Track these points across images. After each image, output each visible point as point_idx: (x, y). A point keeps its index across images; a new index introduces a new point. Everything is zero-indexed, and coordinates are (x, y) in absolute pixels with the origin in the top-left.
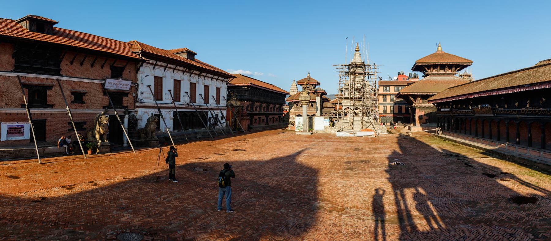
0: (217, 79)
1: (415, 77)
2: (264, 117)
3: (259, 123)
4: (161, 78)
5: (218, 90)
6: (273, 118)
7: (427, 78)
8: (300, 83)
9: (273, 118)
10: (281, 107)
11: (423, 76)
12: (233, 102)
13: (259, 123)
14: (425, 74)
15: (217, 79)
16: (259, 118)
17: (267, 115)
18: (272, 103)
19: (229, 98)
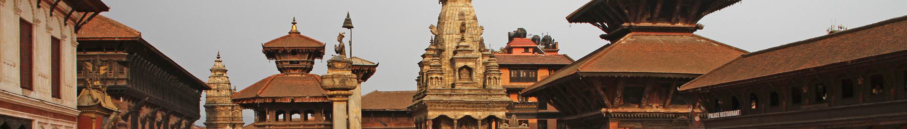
1: (549, 44)
7: (628, 37)
11: (602, 37)
12: (96, 94)
14: (604, 29)
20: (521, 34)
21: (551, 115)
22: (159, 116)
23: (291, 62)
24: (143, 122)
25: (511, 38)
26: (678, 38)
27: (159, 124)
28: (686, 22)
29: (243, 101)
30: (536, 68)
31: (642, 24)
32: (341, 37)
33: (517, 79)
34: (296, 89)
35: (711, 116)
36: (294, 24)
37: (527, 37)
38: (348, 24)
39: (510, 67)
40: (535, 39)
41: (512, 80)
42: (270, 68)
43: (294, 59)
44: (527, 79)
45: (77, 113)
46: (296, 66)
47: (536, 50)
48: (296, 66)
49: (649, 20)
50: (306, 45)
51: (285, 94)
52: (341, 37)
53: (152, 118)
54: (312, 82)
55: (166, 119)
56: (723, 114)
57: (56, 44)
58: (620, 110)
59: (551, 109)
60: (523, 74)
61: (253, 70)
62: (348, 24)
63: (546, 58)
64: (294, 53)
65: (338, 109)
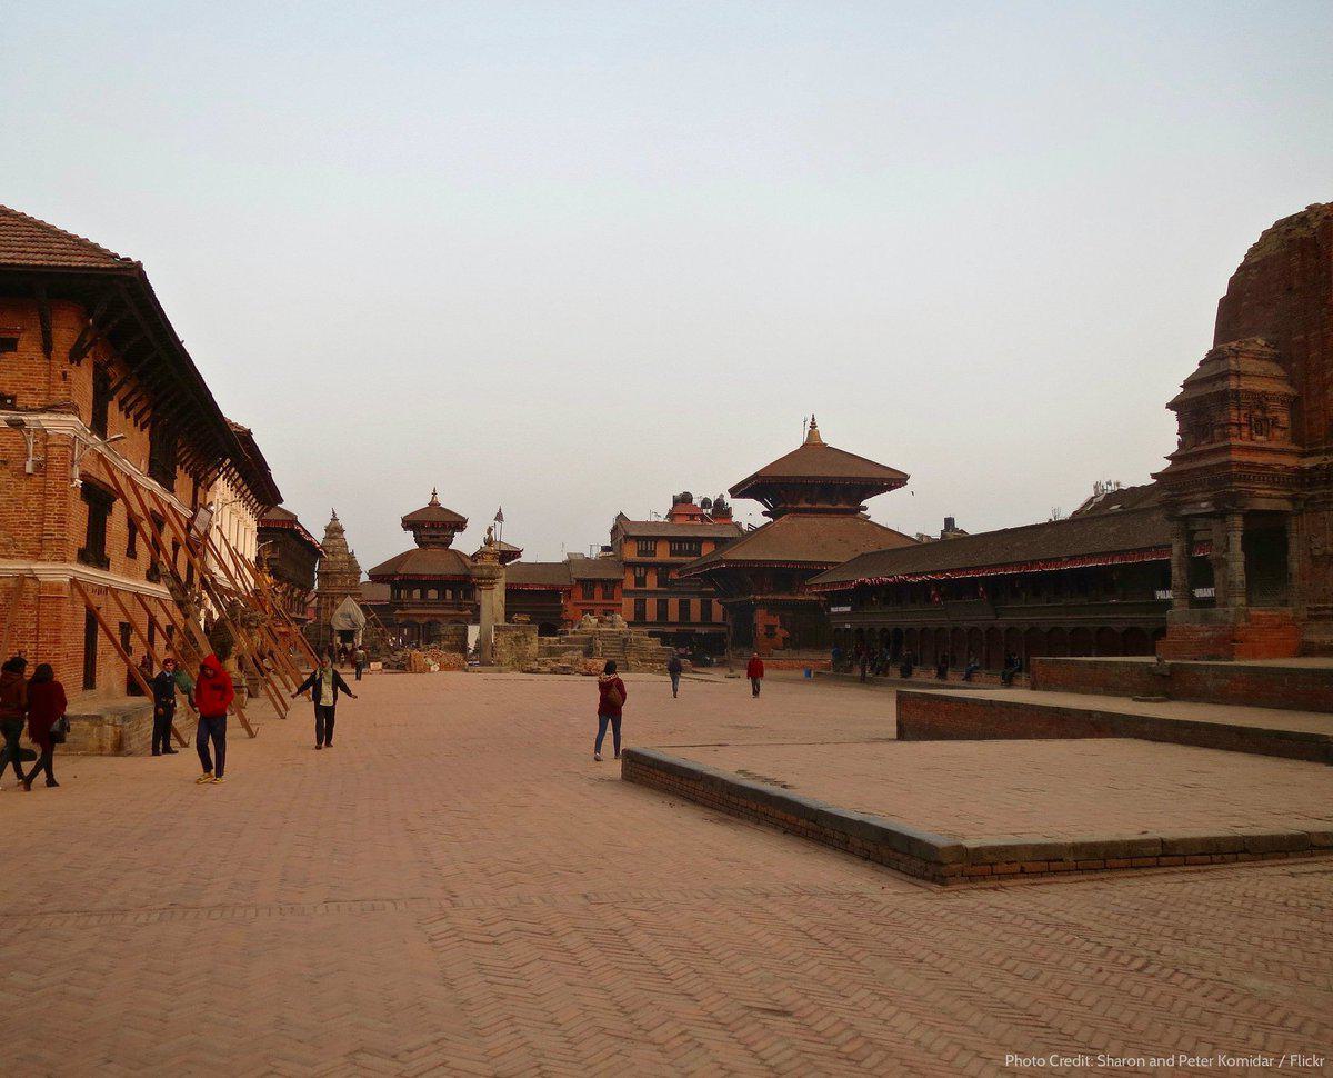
1: (721, 511)
8: (409, 523)
11: (765, 514)
20: (684, 499)
21: (712, 595)
23: (431, 537)
25: (676, 501)
28: (848, 504)
30: (700, 540)
31: (799, 506)
32: (490, 530)
33: (679, 553)
34: (435, 566)
35: (833, 610)
36: (434, 494)
37: (695, 501)
38: (499, 517)
39: (670, 539)
40: (706, 503)
42: (408, 542)
43: (434, 533)
44: (689, 553)
46: (435, 540)
47: (703, 517)
48: (435, 540)
50: (447, 519)
51: (424, 570)
52: (490, 530)
54: (452, 557)
55: (293, 591)
58: (770, 597)
62: (499, 517)
63: (714, 530)
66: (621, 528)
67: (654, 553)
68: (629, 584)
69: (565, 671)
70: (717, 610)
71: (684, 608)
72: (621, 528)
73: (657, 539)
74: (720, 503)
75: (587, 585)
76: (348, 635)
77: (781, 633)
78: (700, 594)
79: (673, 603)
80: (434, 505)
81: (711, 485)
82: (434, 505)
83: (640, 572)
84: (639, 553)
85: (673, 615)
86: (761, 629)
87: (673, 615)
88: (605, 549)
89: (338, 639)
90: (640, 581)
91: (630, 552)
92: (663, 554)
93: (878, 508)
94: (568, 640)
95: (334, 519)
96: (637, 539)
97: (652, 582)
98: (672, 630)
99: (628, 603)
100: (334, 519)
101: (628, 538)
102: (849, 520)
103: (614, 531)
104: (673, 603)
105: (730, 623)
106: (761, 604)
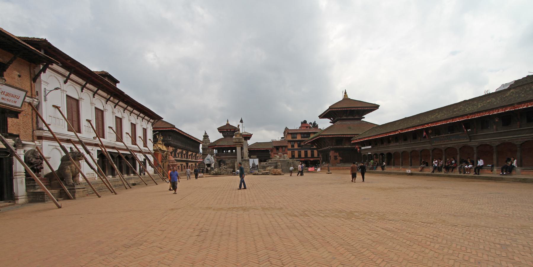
0: (143, 118)
1: (315, 125)
2: (184, 164)
3: (182, 170)
4: (77, 101)
5: (145, 130)
6: (192, 165)
8: (220, 130)
9: (192, 165)
10: (196, 155)
11: (330, 122)
12: (159, 146)
13: (182, 170)
15: (143, 118)
16: (182, 165)
17: (187, 162)
18: (191, 151)
19: (155, 141)
20: (305, 122)
22: (184, 152)
24: (178, 154)
25: (302, 123)
26: (356, 122)
27: (184, 155)
29: (213, 146)
30: (309, 134)
33: (304, 137)
35: (362, 148)
38: (241, 121)
39: (301, 133)
40: (311, 123)
41: (302, 137)
42: (221, 136)
45: (153, 152)
47: (310, 127)
49: (345, 116)
51: (225, 144)
53: (182, 153)
55: (187, 153)
56: (366, 147)
57: (145, 130)
59: (315, 147)
60: (305, 135)
61: (215, 136)
62: (241, 121)
64: (228, 131)
65: (239, 149)
66: (287, 132)
67: (296, 138)
68: (290, 147)
69: (267, 174)
70: (316, 154)
71: (306, 153)
72: (287, 132)
73: (297, 133)
74: (314, 124)
75: (277, 148)
76: (209, 165)
77: (339, 158)
78: (310, 149)
79: (303, 152)
80: (228, 124)
81: (312, 117)
82: (228, 124)
83: (292, 143)
84: (292, 138)
85: (303, 155)
86: (332, 158)
87: (303, 155)
88: (282, 138)
89: (206, 167)
90: (293, 146)
91: (290, 138)
92: (299, 138)
93: (369, 118)
94: (270, 163)
95: (206, 133)
96: (291, 134)
97: (296, 146)
98: (303, 160)
99: (289, 152)
100: (206, 133)
101: (288, 133)
102: (359, 122)
103: (284, 133)
104: (303, 152)
105: (320, 156)
106: (332, 149)
